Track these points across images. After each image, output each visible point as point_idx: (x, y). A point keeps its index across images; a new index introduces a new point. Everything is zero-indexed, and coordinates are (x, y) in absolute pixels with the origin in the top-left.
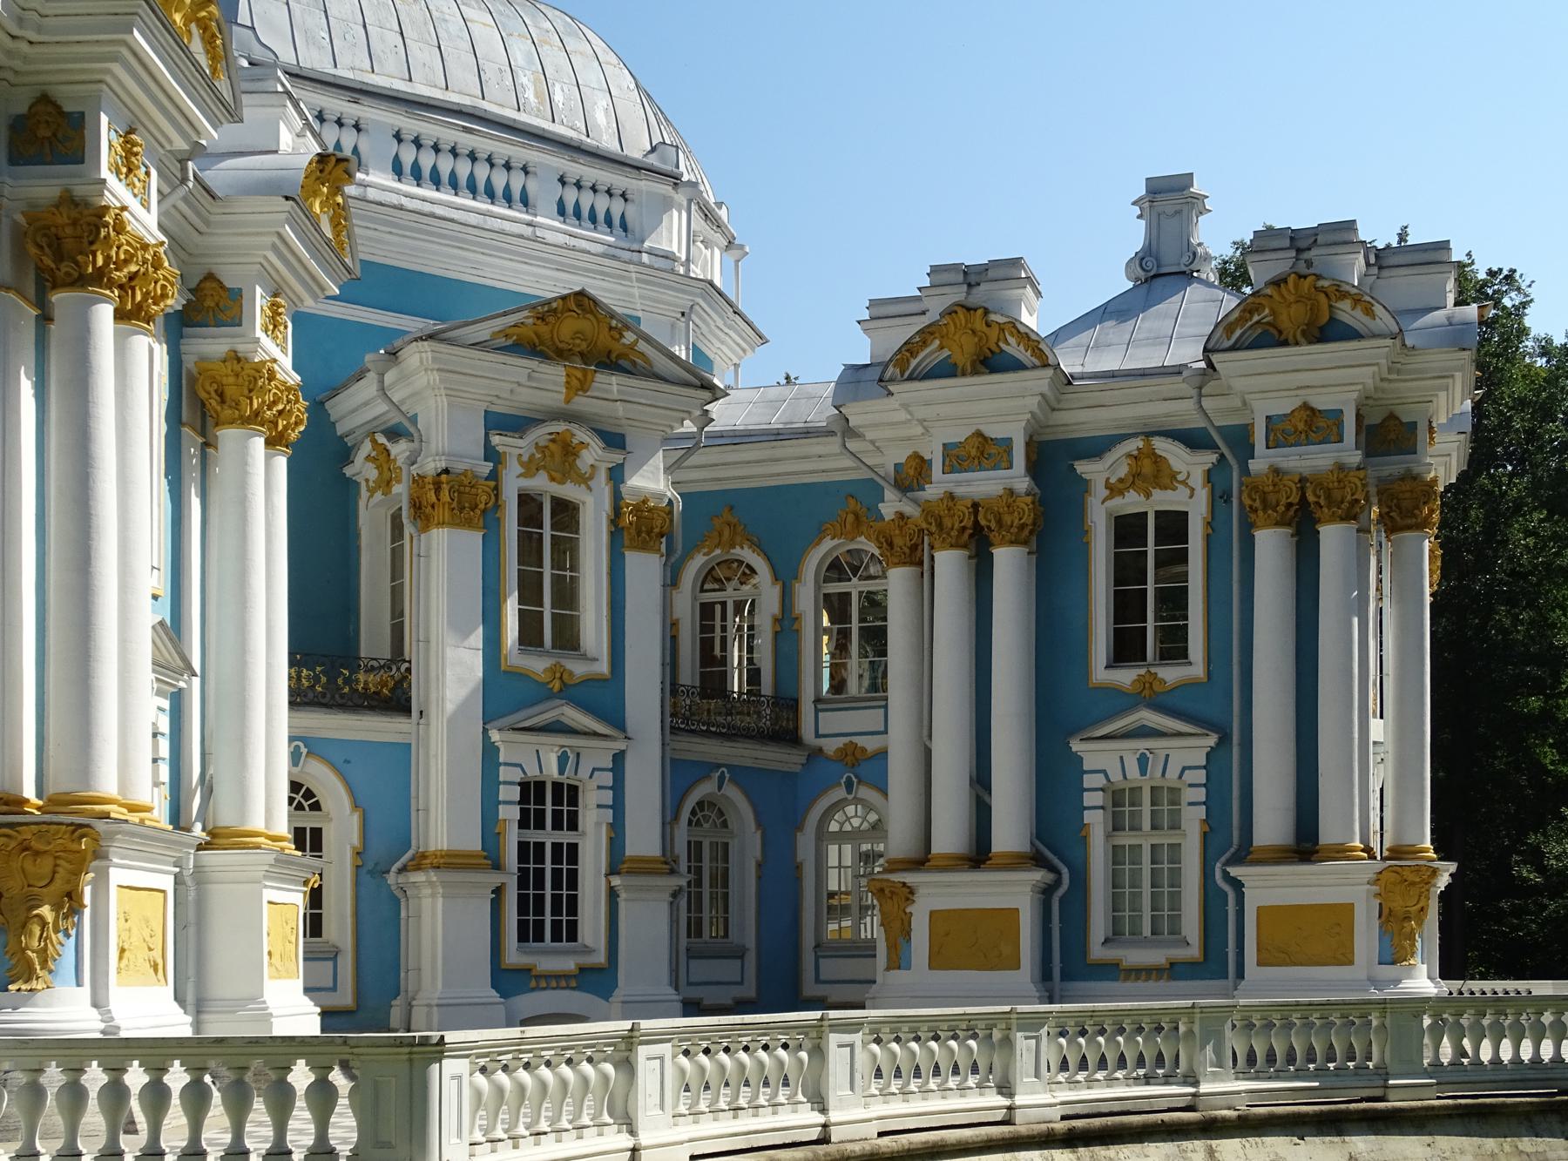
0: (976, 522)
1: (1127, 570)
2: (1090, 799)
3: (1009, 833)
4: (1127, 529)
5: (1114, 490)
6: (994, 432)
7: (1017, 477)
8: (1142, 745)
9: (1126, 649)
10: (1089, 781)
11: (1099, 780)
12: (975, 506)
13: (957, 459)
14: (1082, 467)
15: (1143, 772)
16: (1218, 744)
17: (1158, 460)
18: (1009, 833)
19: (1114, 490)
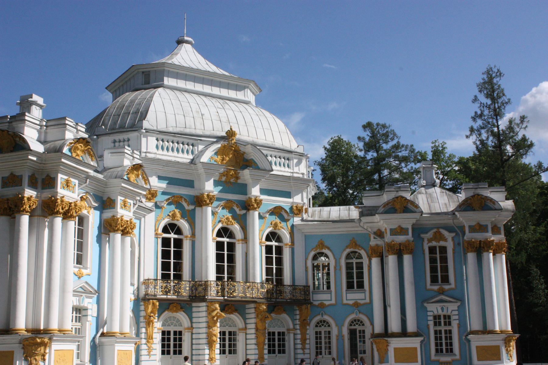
0: (400, 248)
1: (433, 261)
3: (411, 327)
4: (432, 250)
5: (430, 241)
6: (404, 226)
8: (442, 304)
9: (434, 280)
10: (429, 314)
11: (431, 314)
12: (400, 244)
13: (394, 232)
14: (422, 236)
15: (443, 311)
16: (461, 304)
17: (440, 234)
19: (430, 241)
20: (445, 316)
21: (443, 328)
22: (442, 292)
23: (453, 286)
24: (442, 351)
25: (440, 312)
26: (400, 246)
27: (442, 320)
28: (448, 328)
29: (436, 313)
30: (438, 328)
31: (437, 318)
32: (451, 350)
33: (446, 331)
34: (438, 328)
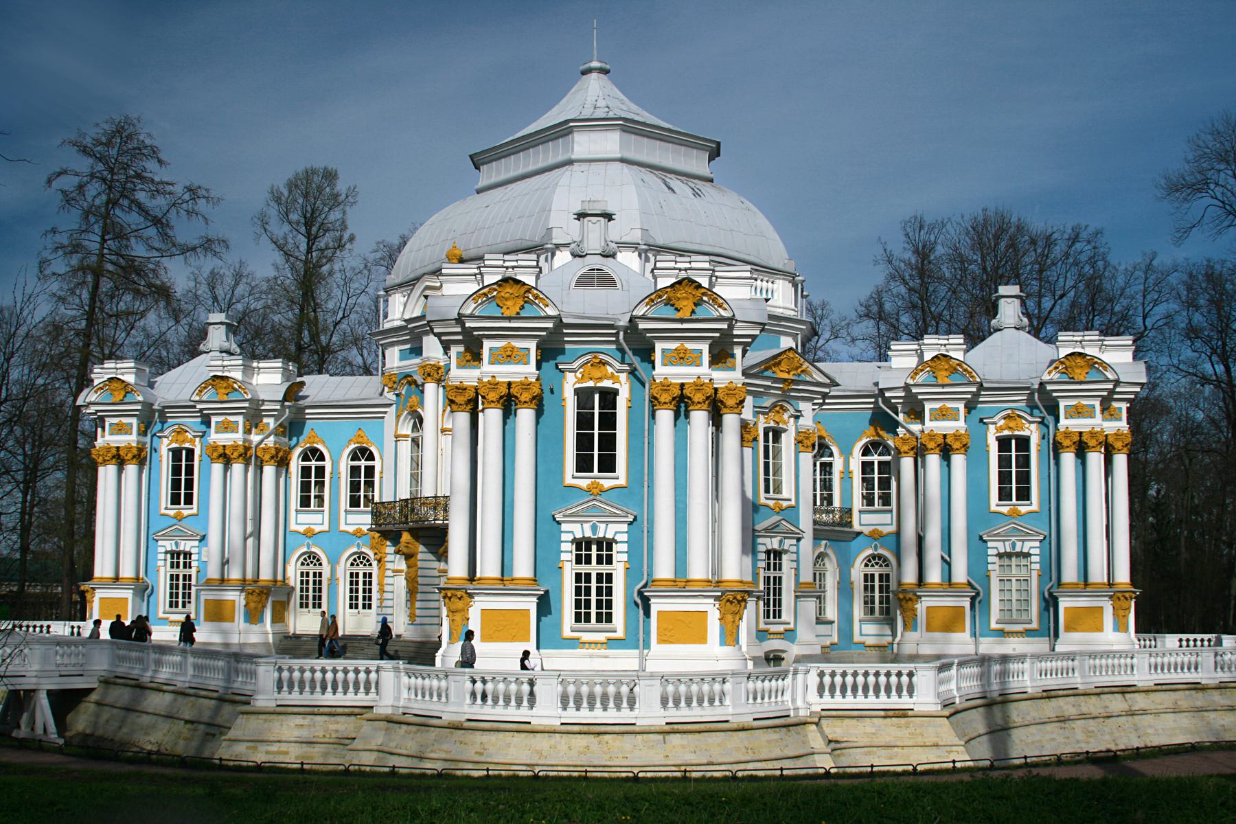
2: (564, 547)
7: (531, 368)
10: (564, 537)
15: (594, 534)
18: (523, 568)
20: (599, 543)
21: (594, 569)
22: (596, 492)
23: (622, 481)
24: (588, 620)
25: (588, 534)
26: (509, 389)
27: (594, 552)
28: (604, 569)
29: (579, 535)
30: (583, 569)
31: (582, 545)
32: (609, 618)
33: (599, 576)
34: (583, 569)
